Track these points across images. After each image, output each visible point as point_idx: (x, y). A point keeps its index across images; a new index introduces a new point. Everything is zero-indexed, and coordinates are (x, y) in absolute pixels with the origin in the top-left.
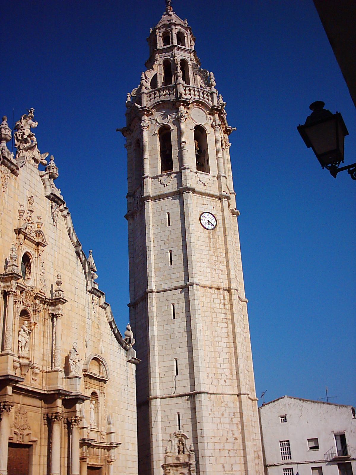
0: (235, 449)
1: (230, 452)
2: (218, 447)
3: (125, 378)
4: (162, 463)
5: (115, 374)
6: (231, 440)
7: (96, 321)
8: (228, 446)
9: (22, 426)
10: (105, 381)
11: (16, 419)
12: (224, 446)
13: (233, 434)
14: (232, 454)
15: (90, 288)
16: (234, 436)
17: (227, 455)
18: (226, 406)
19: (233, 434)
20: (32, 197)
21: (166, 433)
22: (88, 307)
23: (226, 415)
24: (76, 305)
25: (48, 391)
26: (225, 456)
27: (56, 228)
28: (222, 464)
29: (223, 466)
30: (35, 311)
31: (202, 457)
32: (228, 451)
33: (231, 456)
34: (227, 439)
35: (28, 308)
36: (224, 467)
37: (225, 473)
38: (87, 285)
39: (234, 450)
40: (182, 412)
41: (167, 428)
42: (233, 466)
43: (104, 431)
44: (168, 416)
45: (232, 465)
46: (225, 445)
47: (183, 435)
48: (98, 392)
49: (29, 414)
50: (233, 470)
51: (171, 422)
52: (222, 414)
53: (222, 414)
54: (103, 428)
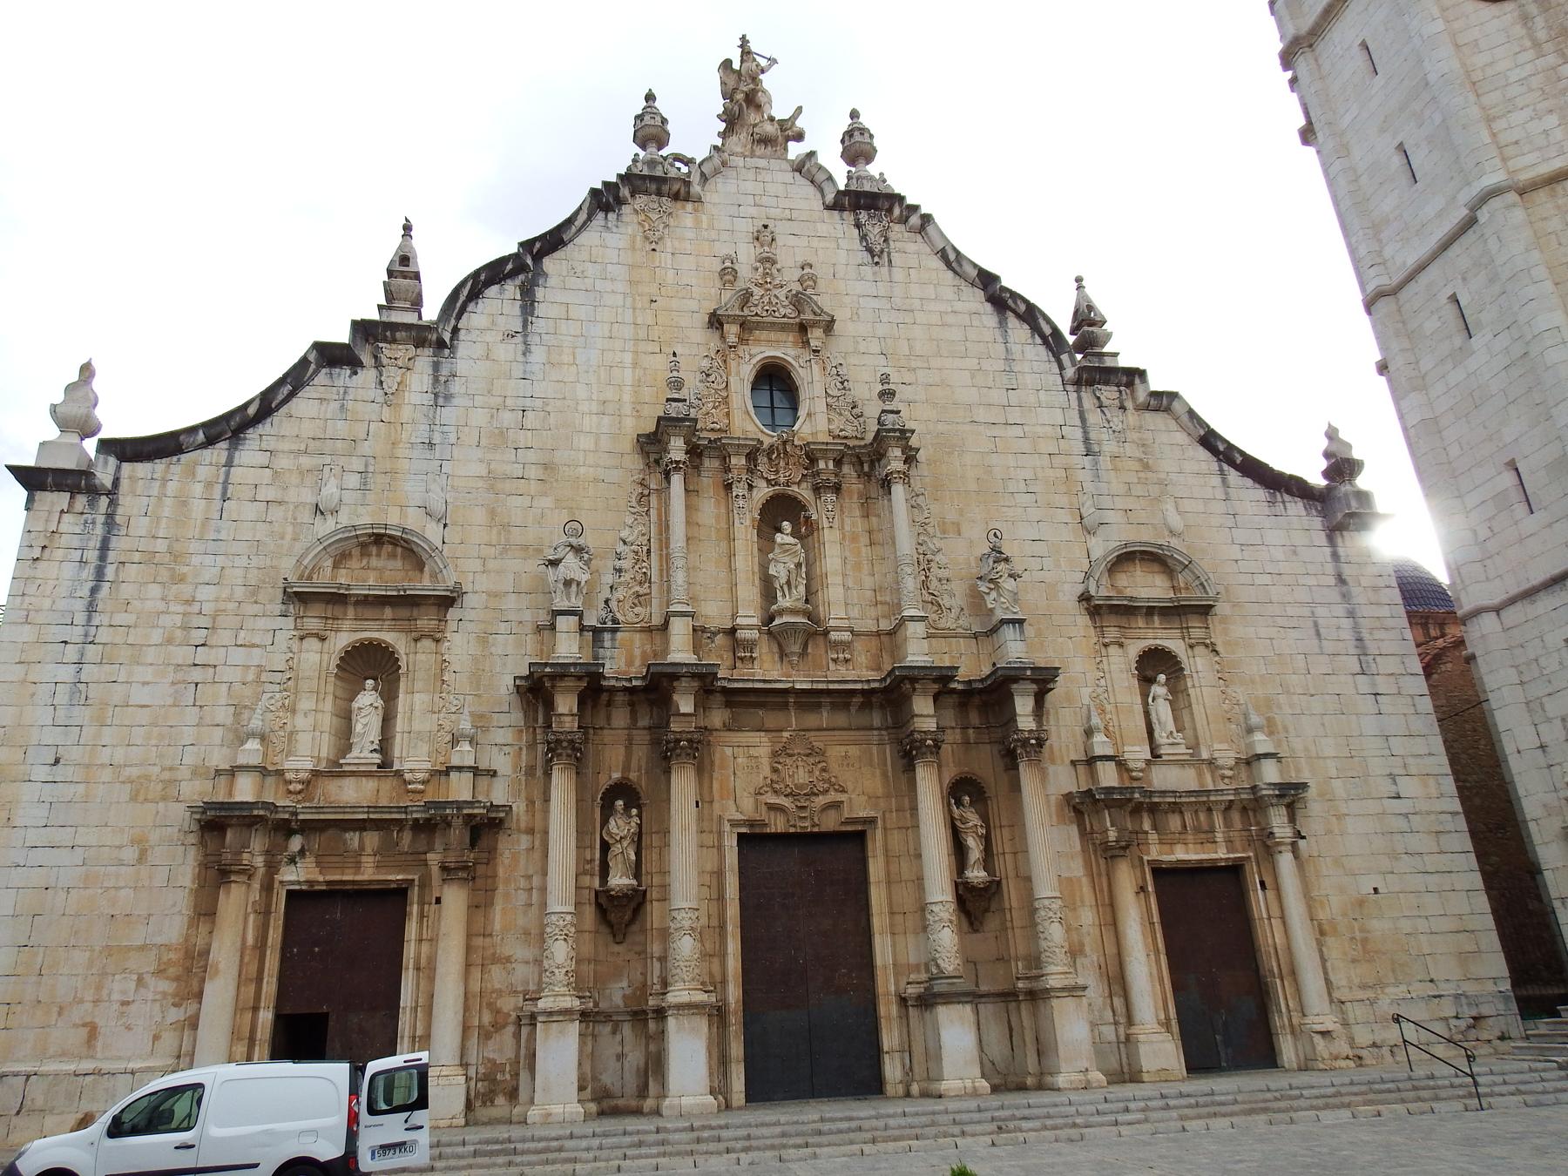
3: (1332, 581)
5: (1260, 579)
7: (1130, 449)
9: (801, 787)
10: (1205, 611)
11: (775, 770)
15: (1070, 372)
20: (766, 227)
21: (1549, 720)
22: (1078, 423)
24: (1018, 431)
25: (880, 681)
27: (885, 270)
30: (817, 490)
35: (795, 488)
38: (1061, 367)
43: (1227, 757)
48: (1176, 645)
49: (835, 752)
54: (1216, 746)
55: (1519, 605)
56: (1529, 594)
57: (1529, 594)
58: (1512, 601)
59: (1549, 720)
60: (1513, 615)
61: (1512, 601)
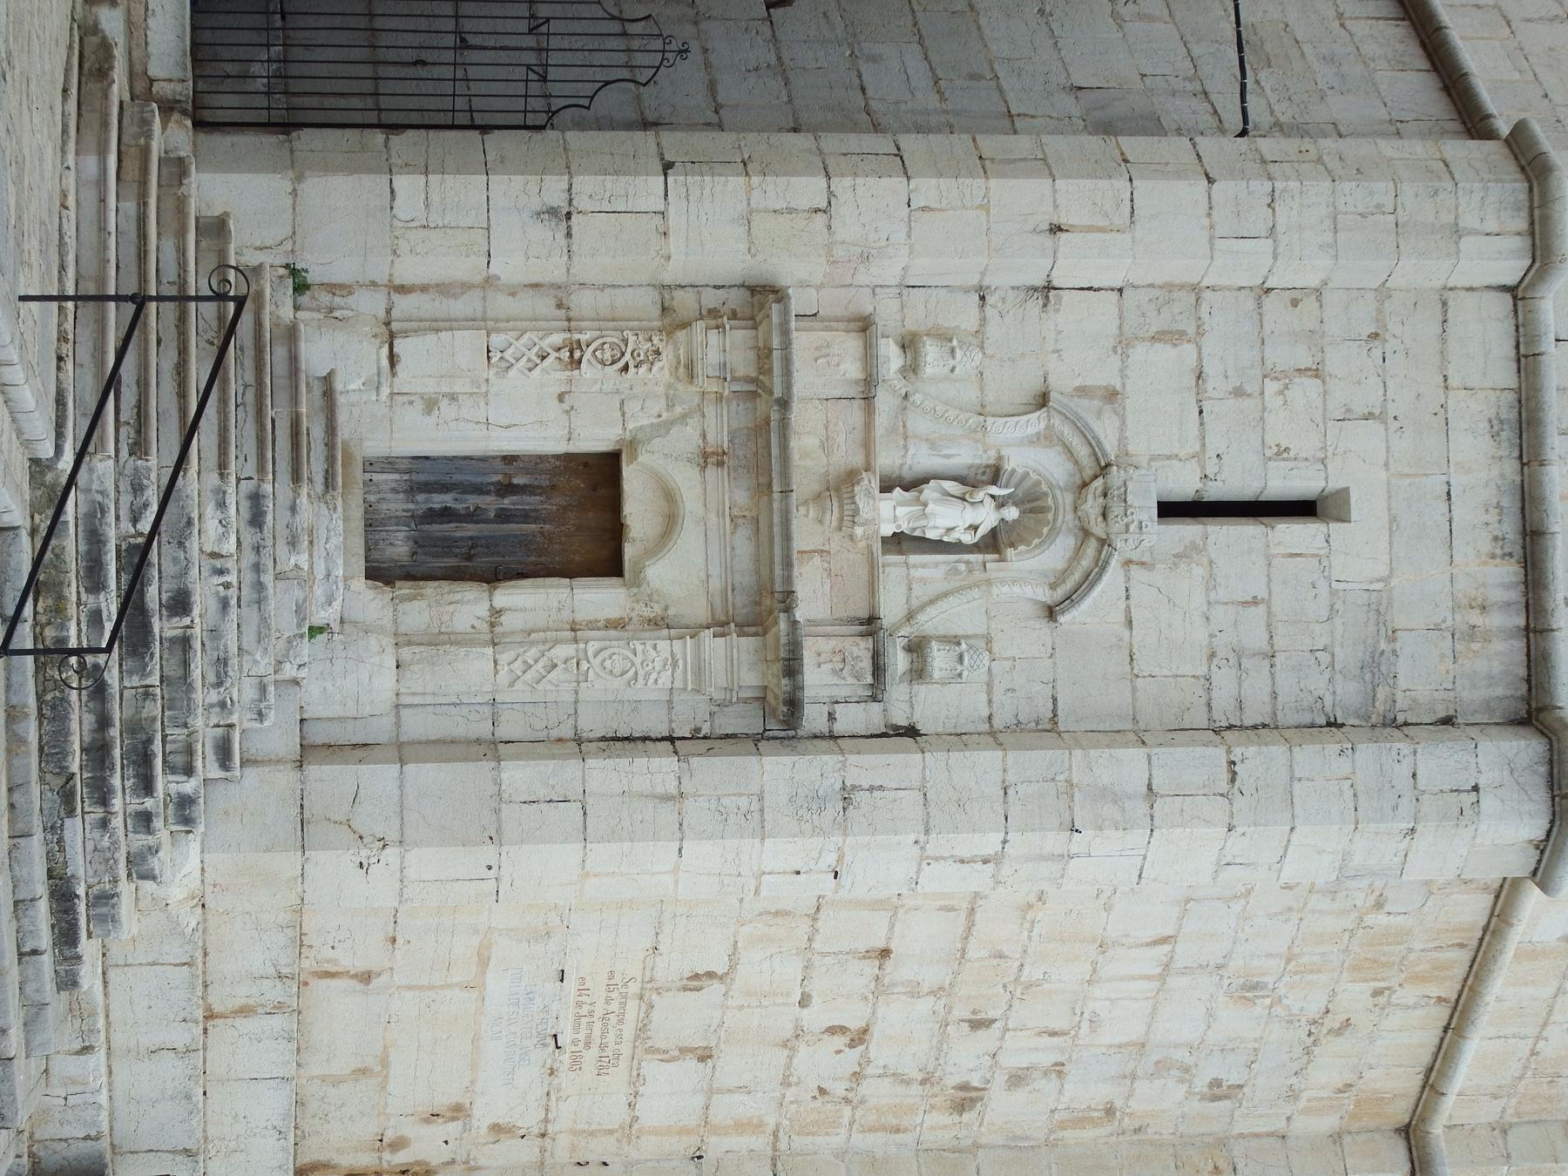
0: (866, 1088)
1: (839, 1041)
2: (922, 941)
4: (799, 269)
6: (966, 1059)
8: (903, 1031)
12: (914, 992)
13: (1017, 1079)
14: (824, 1062)
16: (1000, 1079)
17: (816, 1017)
18: (1333, 1022)
19: (1017, 1079)
21: (1123, 345)
23: (1236, 1021)
26: (804, 1002)
28: (733, 967)
29: (710, 975)
31: (847, 796)
32: (854, 1024)
33: (803, 1050)
34: (977, 1024)
36: (697, 980)
37: (634, 988)
39: (857, 1076)
40: (1352, 552)
41: (1189, 350)
42: (691, 1063)
44: (1316, 372)
45: (705, 1056)
46: (925, 1005)
47: (1097, 548)
50: (651, 1068)
51: (1247, 403)
52: (1251, 990)
53: (1251, 990)
55: (1505, 376)
56: (1525, 428)
57: (1525, 428)
58: (1526, 360)
59: (1123, 345)
60: (1484, 334)
61: (1526, 360)
